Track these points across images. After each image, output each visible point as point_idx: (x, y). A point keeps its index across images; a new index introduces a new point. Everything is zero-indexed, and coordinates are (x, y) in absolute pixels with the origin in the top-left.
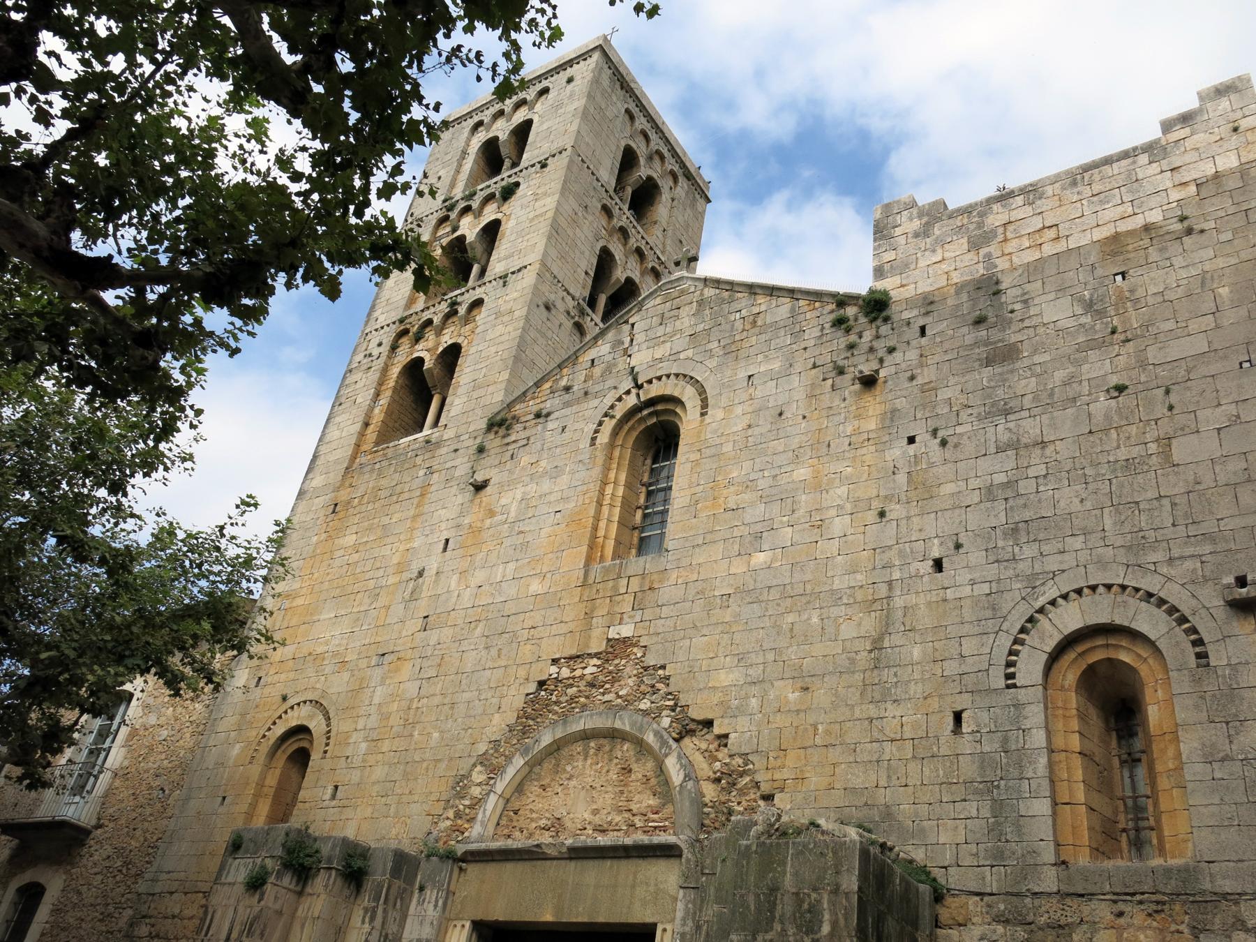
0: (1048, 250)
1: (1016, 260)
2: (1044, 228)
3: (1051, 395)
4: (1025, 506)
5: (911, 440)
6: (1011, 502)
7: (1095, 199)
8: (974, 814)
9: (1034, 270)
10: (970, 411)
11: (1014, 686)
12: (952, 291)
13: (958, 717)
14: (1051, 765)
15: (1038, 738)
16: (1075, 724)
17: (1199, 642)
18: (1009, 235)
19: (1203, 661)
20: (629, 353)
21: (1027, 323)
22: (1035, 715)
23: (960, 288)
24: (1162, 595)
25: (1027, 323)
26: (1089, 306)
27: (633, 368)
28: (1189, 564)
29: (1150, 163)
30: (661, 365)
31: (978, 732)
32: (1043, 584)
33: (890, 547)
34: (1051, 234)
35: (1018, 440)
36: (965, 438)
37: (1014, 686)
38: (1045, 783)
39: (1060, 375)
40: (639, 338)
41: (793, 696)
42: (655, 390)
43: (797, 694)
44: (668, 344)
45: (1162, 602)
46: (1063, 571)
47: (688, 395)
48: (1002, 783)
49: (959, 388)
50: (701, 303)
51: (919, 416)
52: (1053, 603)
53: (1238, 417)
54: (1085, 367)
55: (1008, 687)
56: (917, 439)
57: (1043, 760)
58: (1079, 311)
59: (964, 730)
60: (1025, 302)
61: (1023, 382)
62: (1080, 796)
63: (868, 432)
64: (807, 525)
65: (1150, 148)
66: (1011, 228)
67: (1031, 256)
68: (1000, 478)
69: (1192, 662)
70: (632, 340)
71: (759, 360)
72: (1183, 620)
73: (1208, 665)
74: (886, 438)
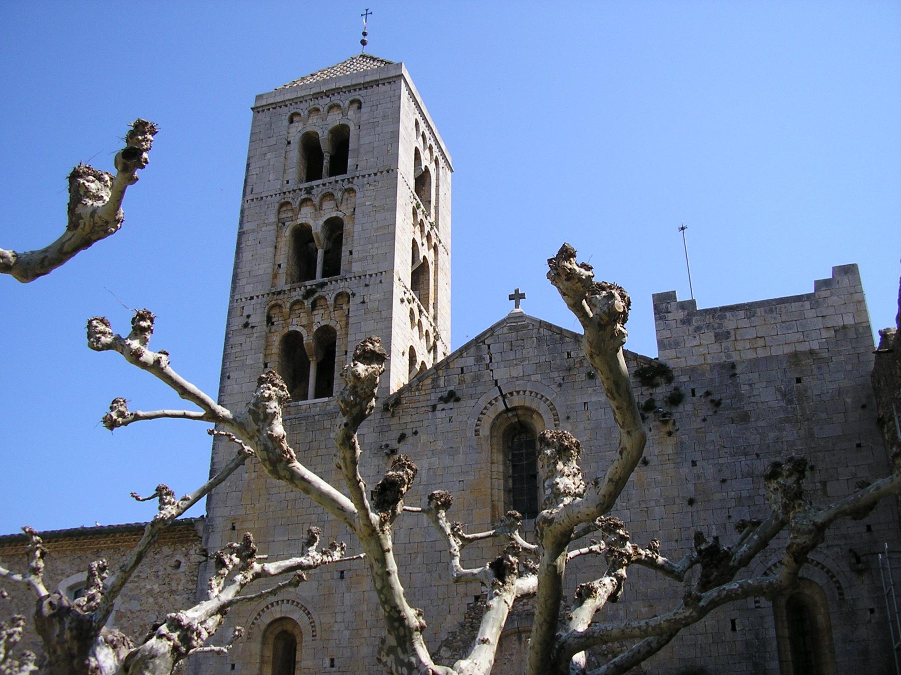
0: (761, 353)
1: (744, 357)
2: (757, 337)
3: (768, 447)
4: (759, 511)
5: (694, 463)
6: (752, 508)
7: (783, 325)
8: (745, 669)
9: (754, 364)
10: (726, 450)
11: (759, 607)
12: (708, 368)
13: (733, 622)
14: (778, 643)
15: (772, 633)
16: (786, 624)
17: (839, 588)
18: (738, 338)
19: (841, 597)
20: (491, 368)
21: (752, 399)
22: (770, 621)
23: (713, 367)
24: (824, 563)
25: (752, 399)
26: (784, 395)
27: (496, 381)
28: (836, 549)
29: (811, 309)
30: (518, 382)
31: (744, 629)
32: (770, 555)
33: (689, 528)
34: (760, 342)
35: (753, 472)
36: (724, 467)
37: (759, 607)
38: (776, 654)
39: (772, 435)
40: (497, 358)
41: (644, 610)
42: (516, 401)
43: (646, 609)
44: (520, 367)
45: (823, 567)
46: (779, 549)
47: (543, 408)
48: (757, 654)
49: (718, 434)
50: (539, 340)
51: (697, 449)
52: (775, 565)
53: (856, 474)
54: (785, 433)
55: (757, 607)
56: (698, 463)
57: (775, 643)
58: (780, 398)
59: (737, 629)
60: (750, 385)
61: (753, 437)
62: (790, 658)
63: (668, 455)
64: (638, 510)
65: (808, 297)
66: (738, 332)
67: (751, 355)
68: (745, 494)
69: (837, 596)
70: (491, 359)
71: (590, 392)
72: (832, 577)
73: (844, 599)
74: (679, 460)
